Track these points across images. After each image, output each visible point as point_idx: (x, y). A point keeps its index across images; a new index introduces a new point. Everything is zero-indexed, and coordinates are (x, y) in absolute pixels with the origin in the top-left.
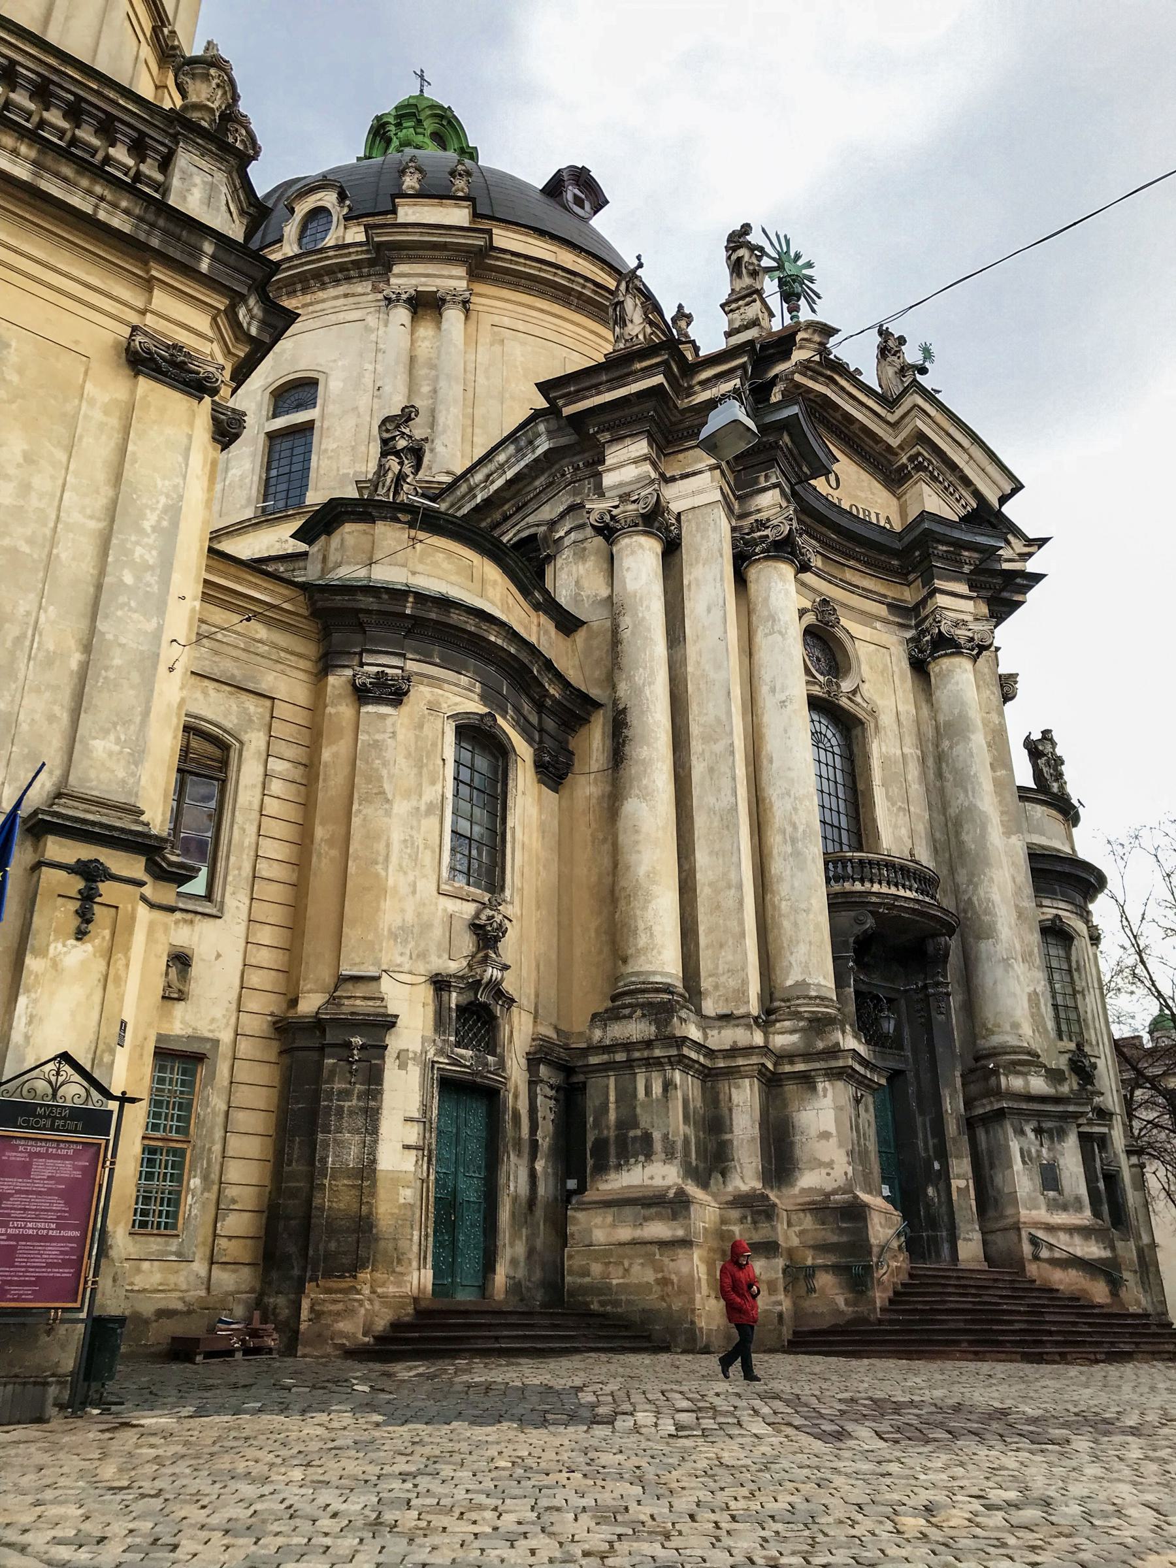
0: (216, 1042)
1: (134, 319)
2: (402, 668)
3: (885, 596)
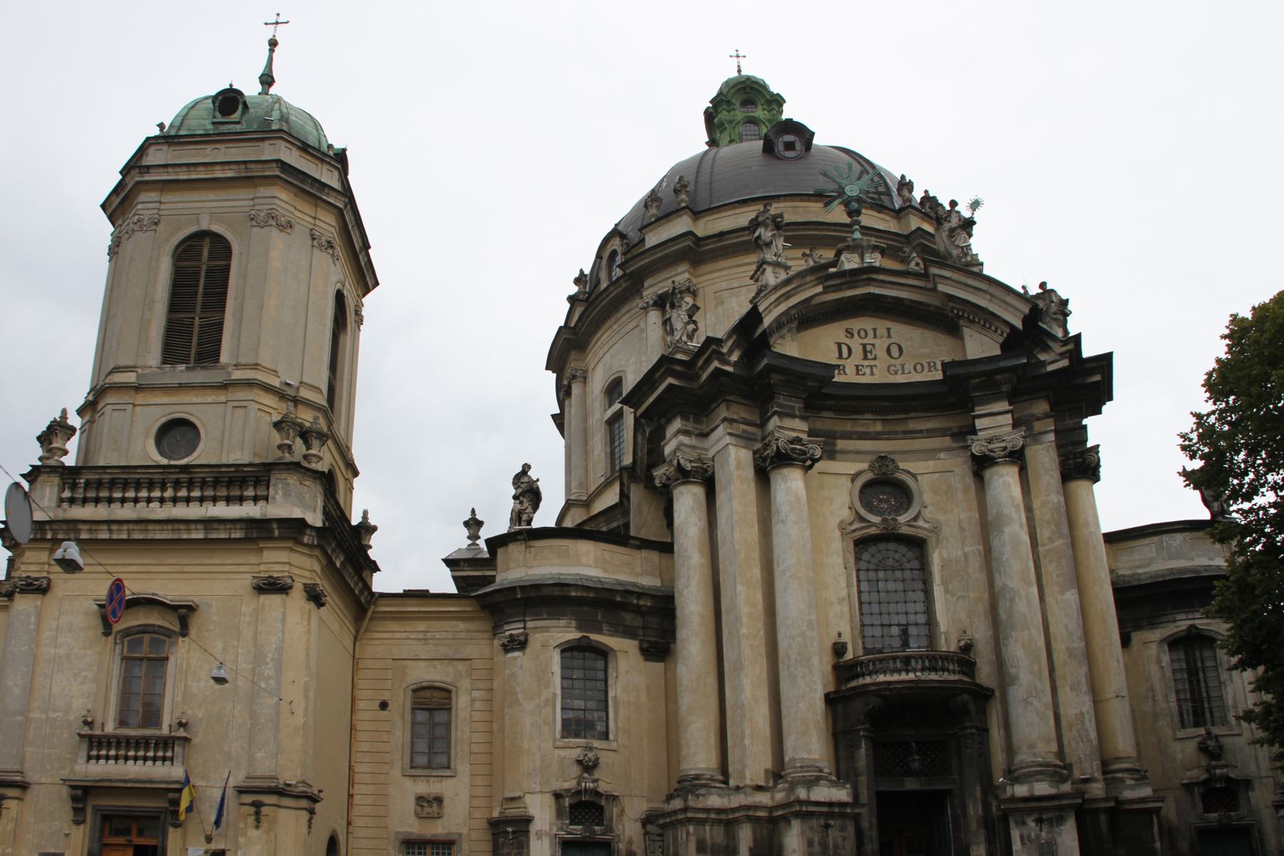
1: (256, 569)
3: (950, 429)
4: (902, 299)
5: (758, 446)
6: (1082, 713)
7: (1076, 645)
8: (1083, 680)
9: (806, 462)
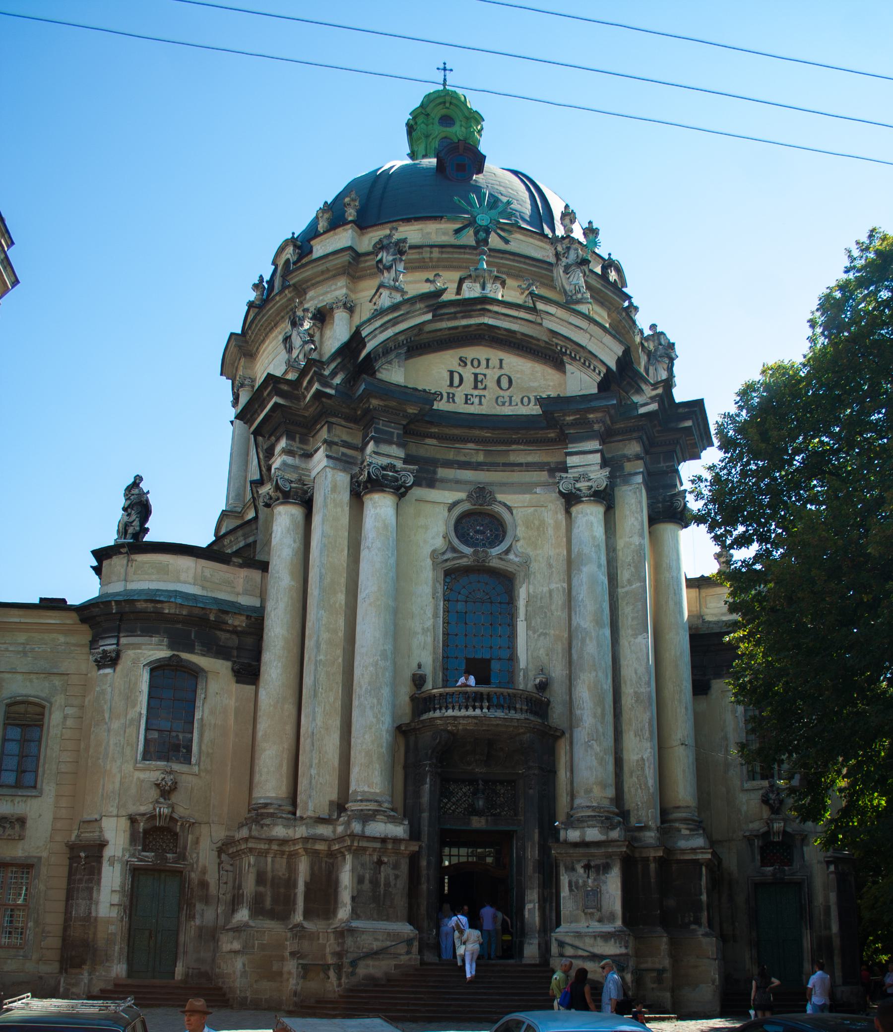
0: (40, 858)
2: (118, 644)
3: (548, 464)
4: (514, 332)
5: (356, 470)
6: (643, 759)
7: (643, 690)
8: (647, 725)
9: (400, 491)
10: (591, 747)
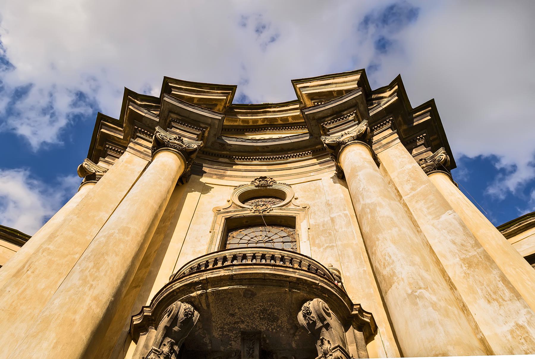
6: (520, 327)
7: (473, 253)
8: (501, 284)
10: (421, 297)
